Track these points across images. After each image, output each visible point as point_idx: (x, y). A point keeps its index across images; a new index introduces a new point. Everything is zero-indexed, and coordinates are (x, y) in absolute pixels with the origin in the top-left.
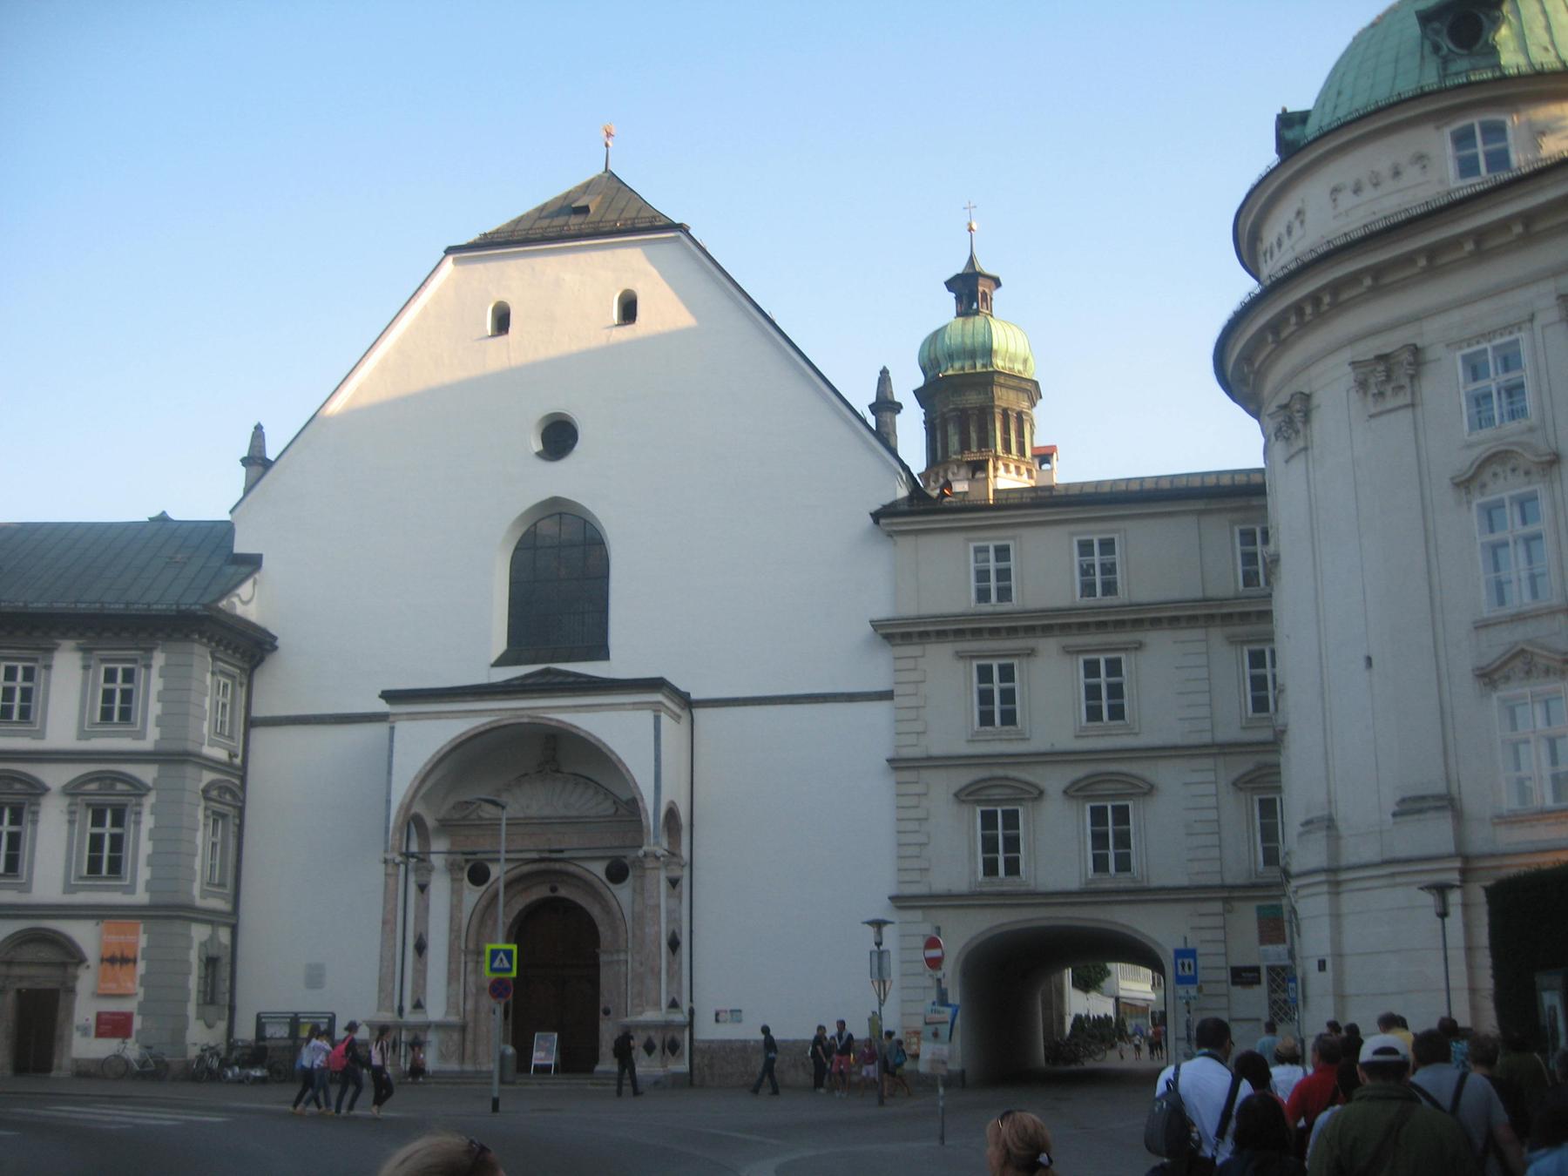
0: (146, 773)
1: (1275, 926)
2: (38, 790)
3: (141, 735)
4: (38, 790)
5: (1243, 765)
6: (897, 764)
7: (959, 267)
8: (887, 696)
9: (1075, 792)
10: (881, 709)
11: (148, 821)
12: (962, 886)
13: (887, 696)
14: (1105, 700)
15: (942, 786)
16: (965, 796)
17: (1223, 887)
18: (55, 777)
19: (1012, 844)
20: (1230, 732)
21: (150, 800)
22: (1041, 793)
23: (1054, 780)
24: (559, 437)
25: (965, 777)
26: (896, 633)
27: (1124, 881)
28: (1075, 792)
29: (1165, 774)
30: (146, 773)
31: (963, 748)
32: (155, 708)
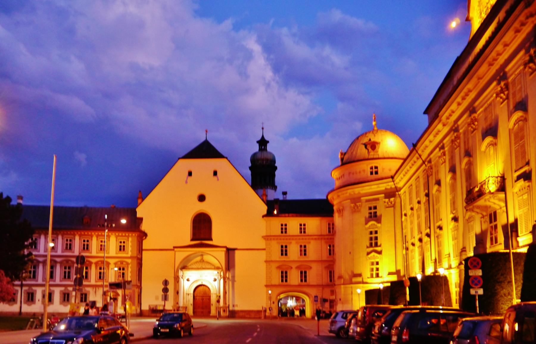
0: (129, 261)
1: (333, 292)
2: (108, 264)
3: (128, 253)
4: (108, 264)
5: (327, 264)
6: (266, 261)
7: (259, 138)
8: (264, 249)
9: (298, 268)
10: (264, 252)
11: (130, 270)
12: (277, 283)
13: (264, 249)
14: (304, 251)
15: (274, 265)
16: (278, 267)
17: (322, 285)
18: (112, 261)
19: (286, 277)
20: (325, 258)
21: (130, 266)
22: (292, 268)
23: (294, 266)
24: (202, 198)
25: (277, 265)
26: (267, 238)
27: (305, 283)
28: (298, 268)
29: (314, 266)
30: (129, 261)
31: (278, 259)
32: (130, 249)
